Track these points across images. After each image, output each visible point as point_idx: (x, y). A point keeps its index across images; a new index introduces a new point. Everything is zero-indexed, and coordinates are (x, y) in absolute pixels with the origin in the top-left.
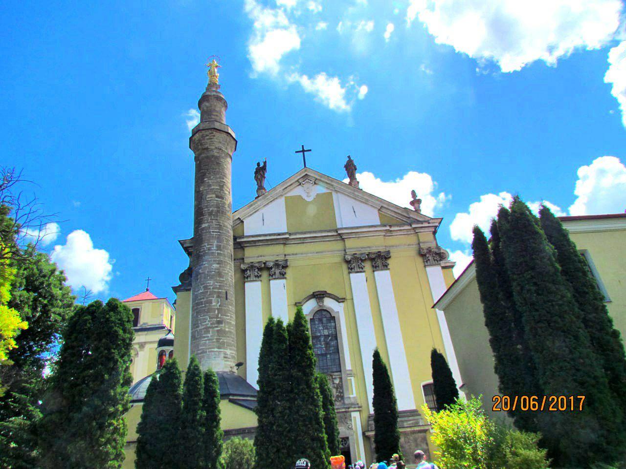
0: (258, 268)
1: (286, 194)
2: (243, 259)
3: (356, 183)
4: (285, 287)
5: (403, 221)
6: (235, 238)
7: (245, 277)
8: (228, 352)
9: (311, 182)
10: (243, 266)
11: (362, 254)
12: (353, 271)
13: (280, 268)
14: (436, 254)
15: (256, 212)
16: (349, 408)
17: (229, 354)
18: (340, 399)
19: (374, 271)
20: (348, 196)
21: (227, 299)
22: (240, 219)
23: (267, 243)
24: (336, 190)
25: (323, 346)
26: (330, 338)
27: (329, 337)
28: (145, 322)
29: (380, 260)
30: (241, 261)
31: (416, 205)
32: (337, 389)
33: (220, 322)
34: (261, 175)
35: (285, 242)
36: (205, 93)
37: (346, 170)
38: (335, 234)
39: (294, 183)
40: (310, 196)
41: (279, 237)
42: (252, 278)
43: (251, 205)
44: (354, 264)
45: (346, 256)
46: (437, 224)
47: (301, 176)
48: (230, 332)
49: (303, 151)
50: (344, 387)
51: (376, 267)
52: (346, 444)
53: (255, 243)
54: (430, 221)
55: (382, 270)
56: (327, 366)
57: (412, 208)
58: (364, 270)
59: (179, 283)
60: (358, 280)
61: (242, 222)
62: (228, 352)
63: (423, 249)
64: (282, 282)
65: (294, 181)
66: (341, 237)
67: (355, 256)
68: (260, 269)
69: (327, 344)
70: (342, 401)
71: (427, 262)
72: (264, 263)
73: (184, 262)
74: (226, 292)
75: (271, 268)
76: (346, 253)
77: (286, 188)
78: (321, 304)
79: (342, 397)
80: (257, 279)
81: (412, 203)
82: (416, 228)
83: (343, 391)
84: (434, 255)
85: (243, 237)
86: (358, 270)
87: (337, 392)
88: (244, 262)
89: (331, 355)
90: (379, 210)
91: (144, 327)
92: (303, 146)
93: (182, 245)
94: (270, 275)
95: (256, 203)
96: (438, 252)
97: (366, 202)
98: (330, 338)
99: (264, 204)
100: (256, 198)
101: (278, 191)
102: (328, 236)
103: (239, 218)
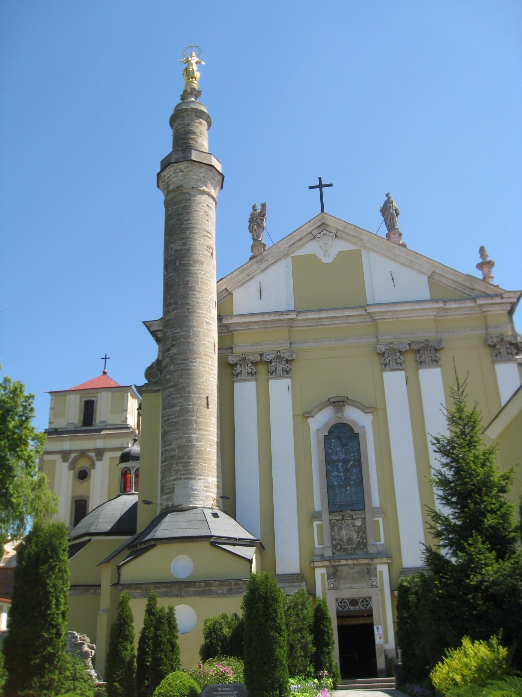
0: (252, 363)
1: (293, 252)
2: (231, 348)
3: (397, 235)
4: (290, 389)
5: (464, 293)
7: (233, 374)
9: (331, 235)
10: (231, 360)
11: (402, 343)
12: (387, 367)
13: (284, 362)
14: (511, 344)
15: (250, 279)
16: (372, 559)
17: (211, 482)
18: (362, 547)
19: (418, 369)
20: (384, 255)
21: (208, 407)
22: (228, 291)
23: (265, 326)
24: (366, 248)
25: (342, 474)
26: (351, 463)
27: (350, 461)
28: (103, 419)
29: (426, 352)
30: (230, 351)
31: (486, 269)
32: (358, 533)
34: (258, 224)
35: (290, 324)
36: (179, 105)
37: (383, 215)
38: (364, 313)
39: (305, 236)
40: (328, 256)
41: (282, 317)
42: (244, 375)
43: (244, 270)
44: (389, 358)
45: (379, 346)
46: (515, 300)
47: (316, 226)
49: (321, 186)
50: (368, 530)
51: (421, 363)
52: (367, 605)
53: (249, 326)
54: (505, 295)
55: (430, 367)
56: (346, 502)
57: (479, 274)
58: (403, 367)
59: (142, 381)
60: (394, 382)
61: (231, 294)
63: (491, 337)
64: (286, 382)
65: (305, 234)
66: (372, 317)
67: (391, 346)
68: (255, 364)
69: (347, 471)
70: (365, 550)
71: (496, 355)
72: (261, 355)
73: (150, 352)
74: (207, 397)
75: (271, 362)
76: (378, 341)
77: (294, 243)
78: (340, 416)
79: (365, 545)
80: (250, 377)
81: (480, 266)
82: (483, 305)
83: (366, 535)
84: (508, 346)
85: (232, 316)
86: (395, 367)
87: (358, 538)
88: (232, 352)
89: (350, 487)
90: (429, 277)
92: (320, 179)
93: (148, 328)
94: (269, 372)
95: (251, 266)
96: (513, 342)
97: (411, 265)
98: (351, 463)
99: (262, 269)
100: (251, 259)
101: (283, 249)
102: (351, 316)
103: (226, 289)
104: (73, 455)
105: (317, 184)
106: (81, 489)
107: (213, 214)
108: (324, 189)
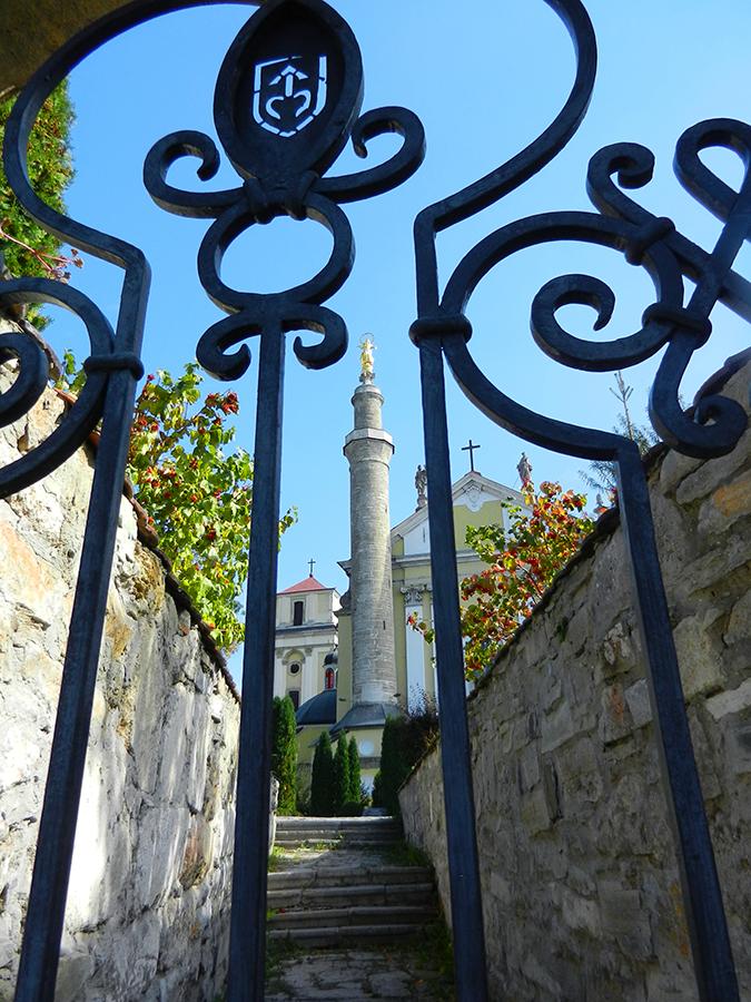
6: (393, 559)
8: (387, 682)
10: (403, 590)
33: (378, 653)
48: (390, 663)
49: (471, 448)
62: (387, 682)
91: (309, 625)
100: (417, 510)
104: (286, 651)
105: (468, 446)
106: (294, 685)
107: (387, 479)
108: (474, 450)
